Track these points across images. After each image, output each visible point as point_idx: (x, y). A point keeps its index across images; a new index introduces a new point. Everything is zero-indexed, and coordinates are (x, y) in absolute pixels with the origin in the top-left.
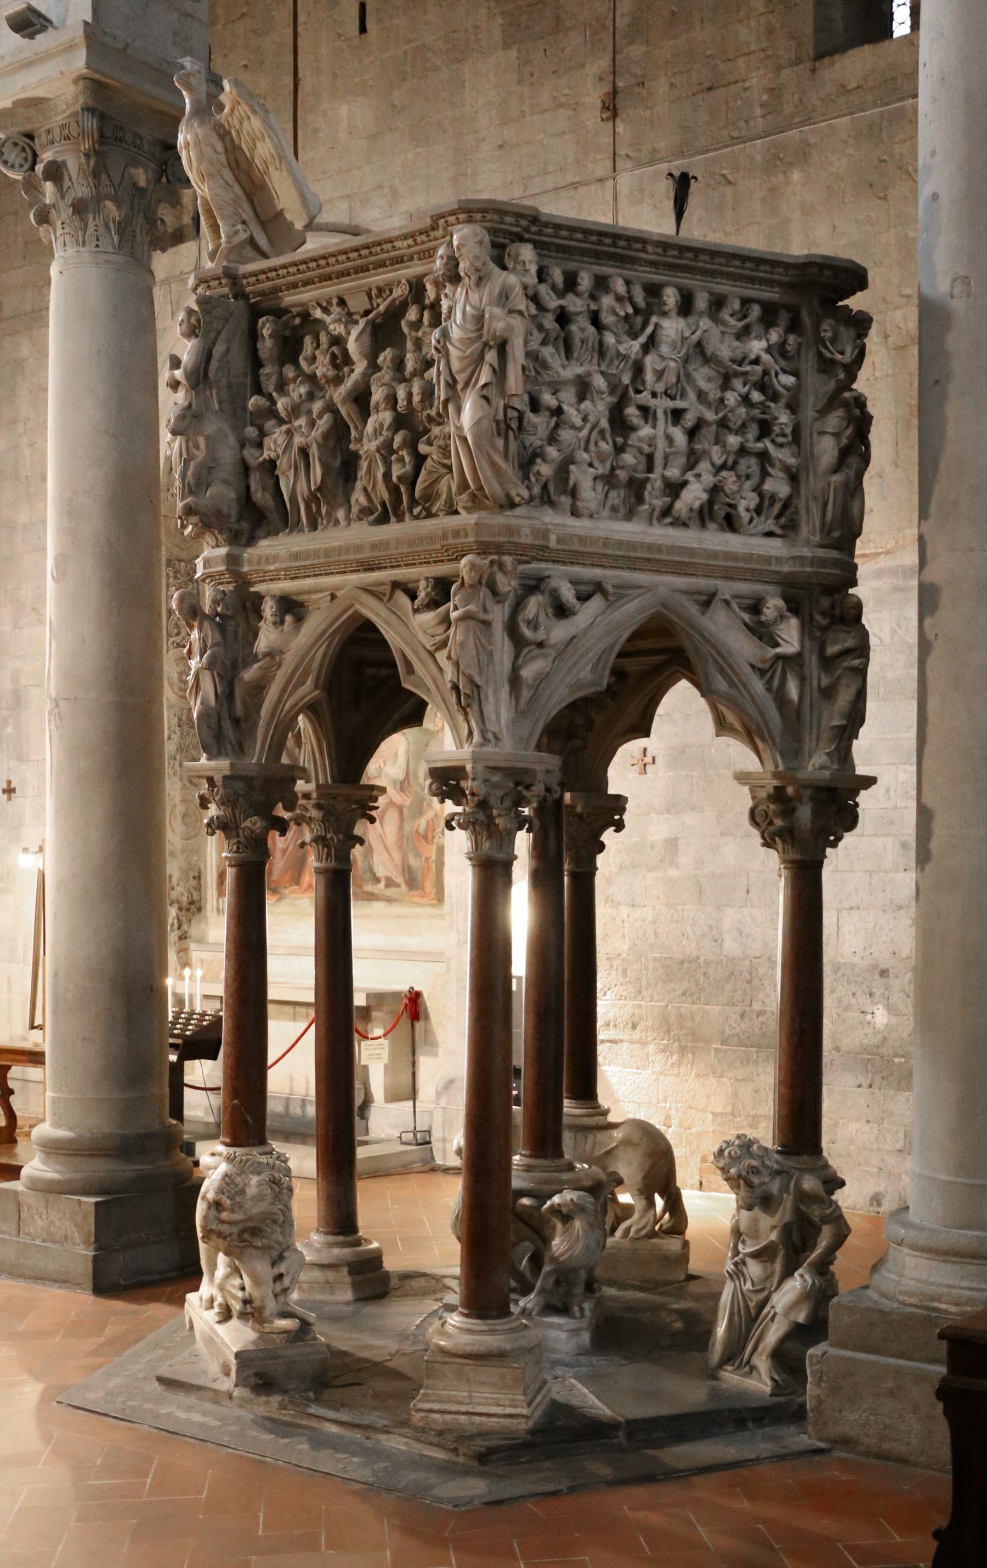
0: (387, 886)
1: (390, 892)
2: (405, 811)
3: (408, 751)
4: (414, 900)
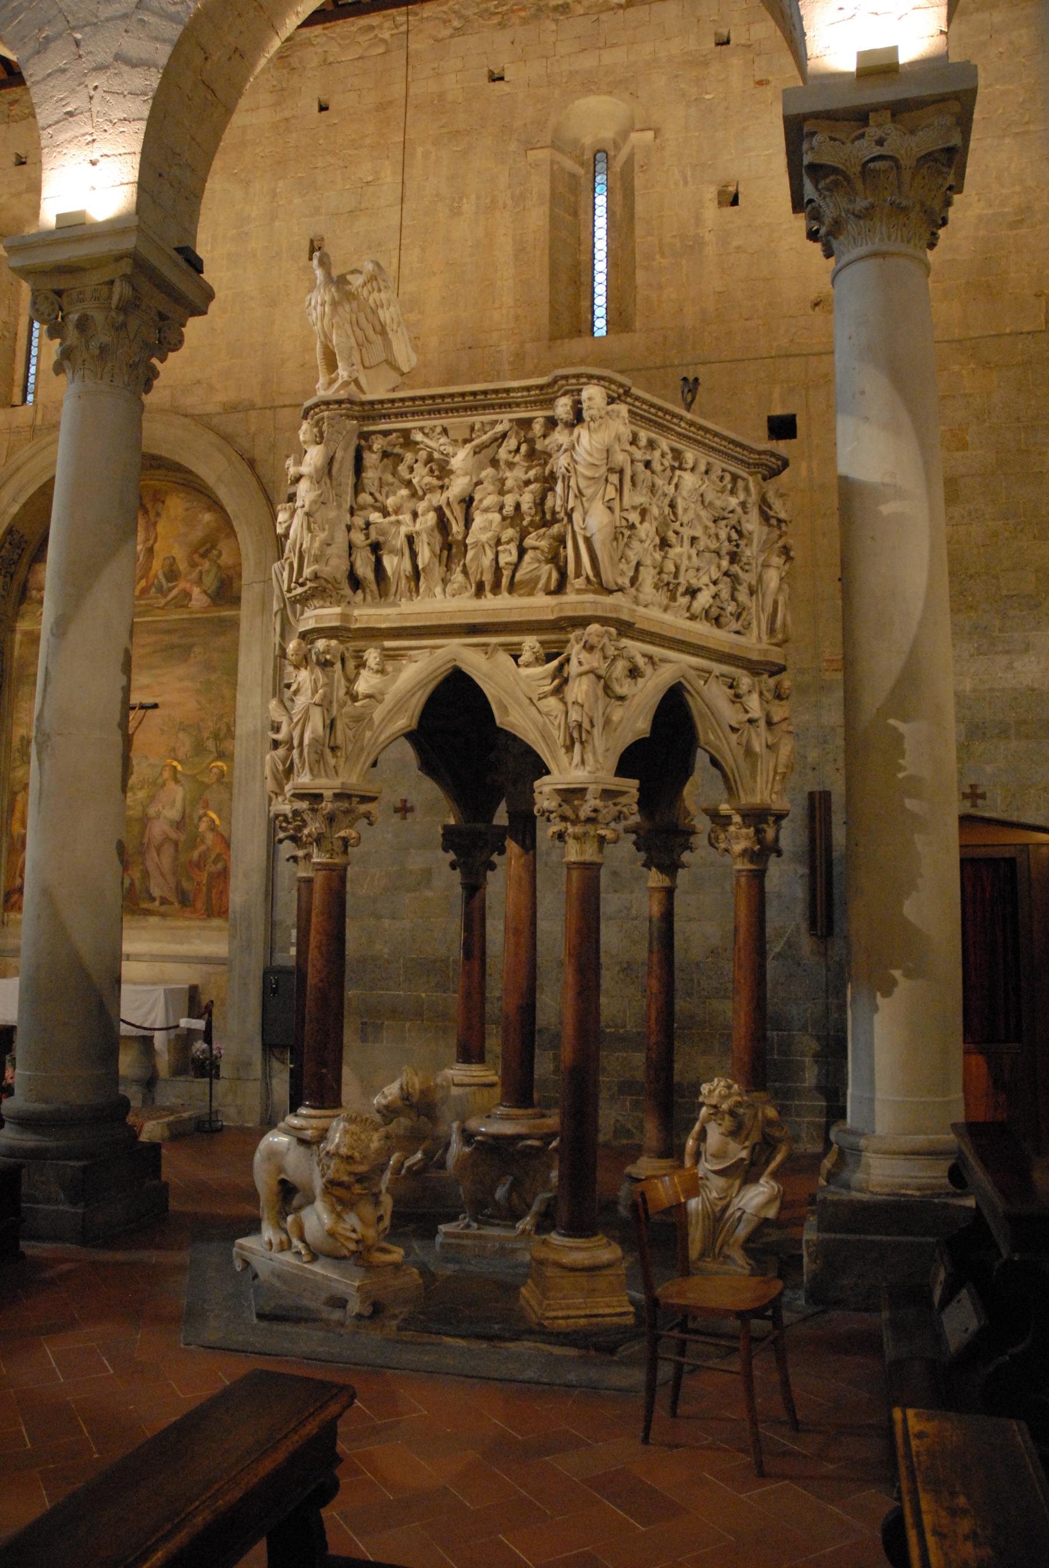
1: (163, 909)
2: (180, 846)
3: (184, 799)
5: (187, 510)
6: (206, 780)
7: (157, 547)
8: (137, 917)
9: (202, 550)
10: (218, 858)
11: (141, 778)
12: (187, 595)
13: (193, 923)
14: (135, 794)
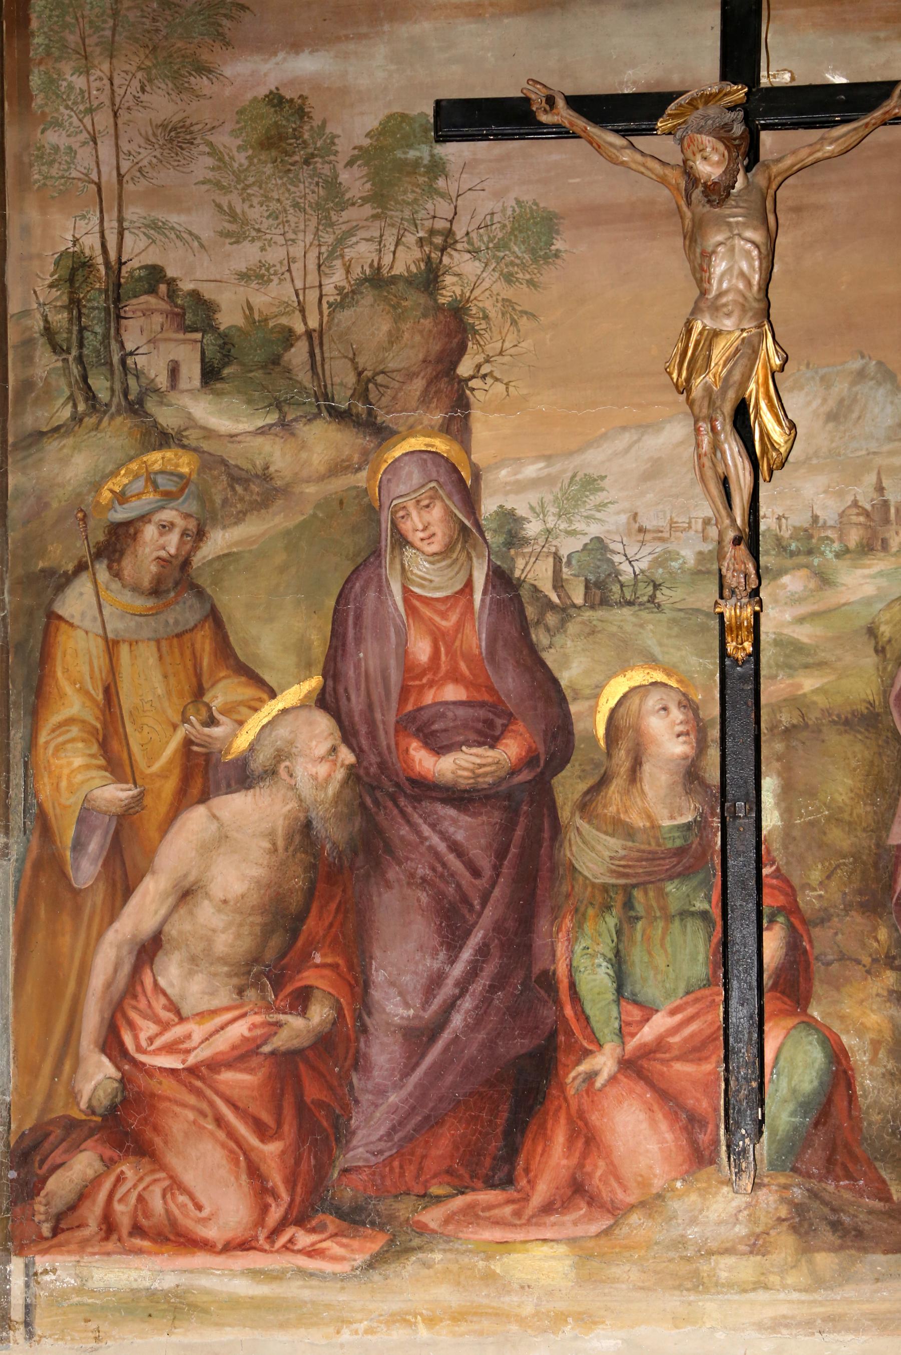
14: (824, 580)
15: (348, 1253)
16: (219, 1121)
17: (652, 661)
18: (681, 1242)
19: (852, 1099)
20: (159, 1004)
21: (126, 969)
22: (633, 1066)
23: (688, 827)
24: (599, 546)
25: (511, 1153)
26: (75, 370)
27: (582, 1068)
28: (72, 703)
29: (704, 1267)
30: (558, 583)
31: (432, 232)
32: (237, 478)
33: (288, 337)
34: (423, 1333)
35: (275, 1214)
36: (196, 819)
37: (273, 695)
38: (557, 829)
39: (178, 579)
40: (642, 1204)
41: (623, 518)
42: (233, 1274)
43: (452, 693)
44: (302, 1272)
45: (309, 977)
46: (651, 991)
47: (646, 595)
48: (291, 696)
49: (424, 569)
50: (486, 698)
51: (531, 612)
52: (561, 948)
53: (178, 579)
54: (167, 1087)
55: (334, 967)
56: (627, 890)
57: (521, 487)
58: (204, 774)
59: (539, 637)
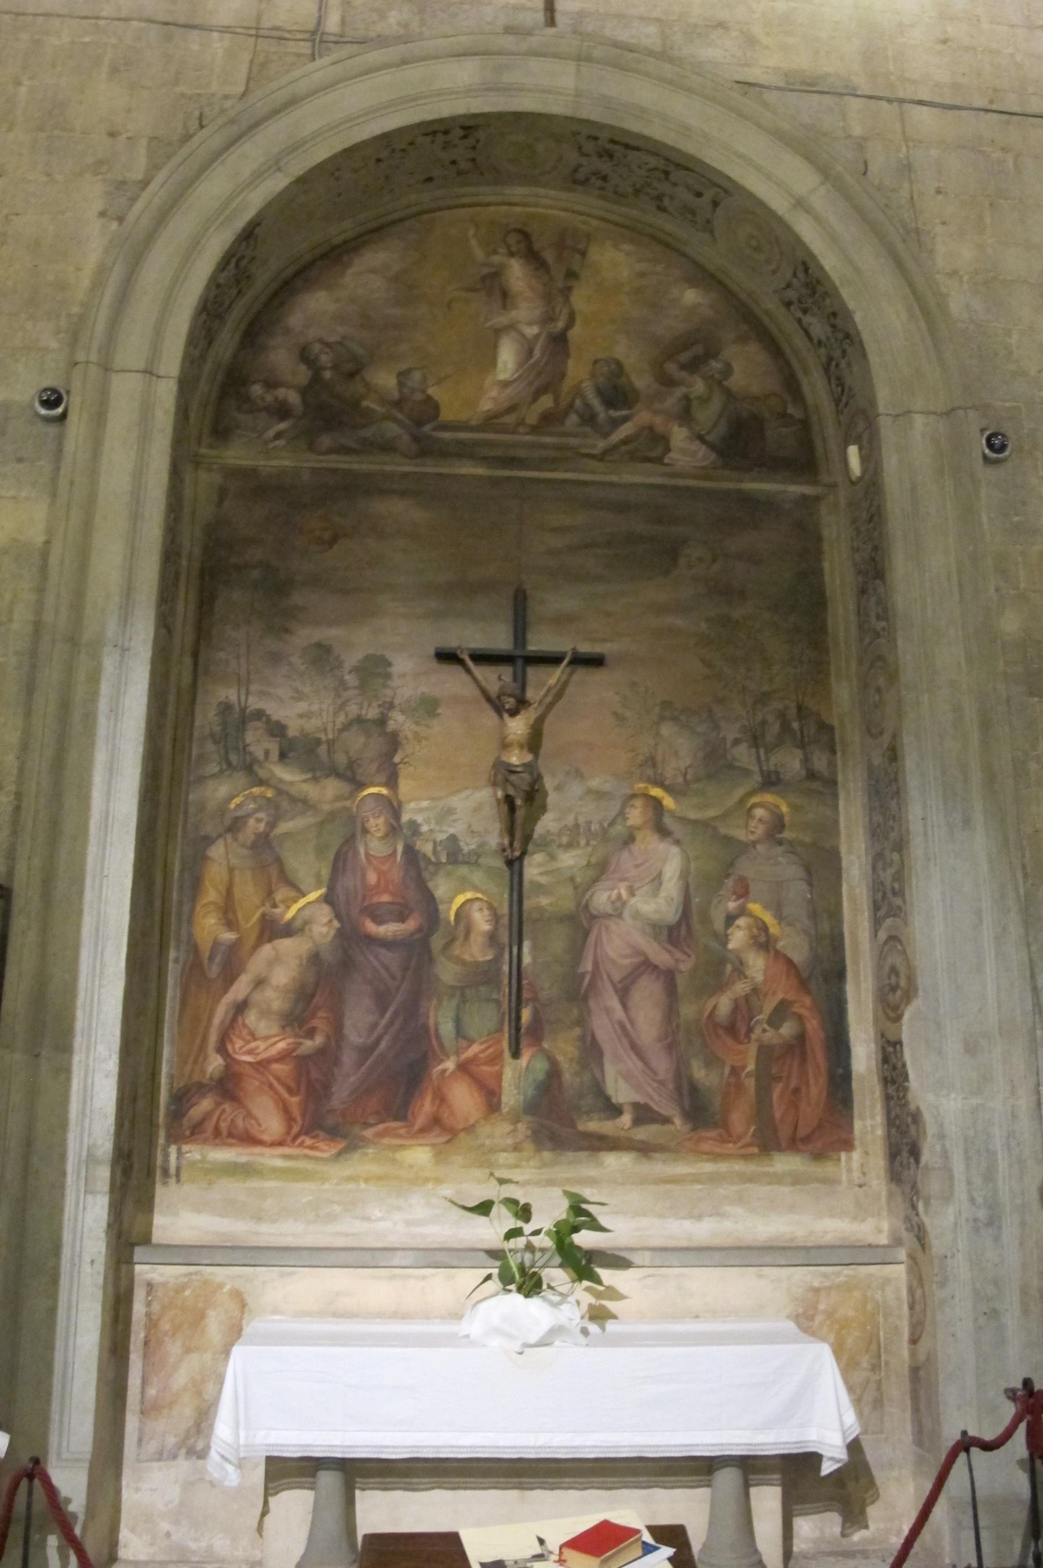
0: (637, 1121)
1: (642, 1133)
2: (681, 981)
3: (684, 875)
4: (705, 1146)
5: (642, 275)
6: (740, 834)
7: (575, 334)
8: (571, 1155)
9: (684, 357)
10: (781, 1013)
11: (570, 820)
12: (662, 440)
13: (723, 1167)
14: (552, 857)
15: (327, 1150)
16: (271, 1086)
17: (475, 888)
18: (482, 1145)
19: (560, 1085)
20: (245, 1032)
21: (230, 1016)
22: (463, 1068)
23: (490, 961)
24: (453, 838)
25: (406, 1104)
26: (222, 752)
27: (440, 1067)
28: (211, 895)
29: (493, 1158)
30: (435, 852)
31: (384, 702)
32: (293, 800)
33: (318, 742)
34: (363, 1185)
35: (296, 1129)
36: (267, 950)
37: (304, 895)
38: (431, 960)
39: (263, 843)
40: (465, 1129)
41: (465, 826)
42: (274, 1156)
43: (385, 898)
44: (307, 1157)
45: (315, 1023)
46: (472, 1033)
47: (473, 860)
48: (313, 896)
49: (375, 845)
50: (400, 900)
51: (422, 864)
52: (432, 1014)
53: (263, 843)
54: (248, 1070)
55: (326, 1018)
56: (462, 988)
57: (421, 810)
58: (272, 929)
59: (426, 875)
